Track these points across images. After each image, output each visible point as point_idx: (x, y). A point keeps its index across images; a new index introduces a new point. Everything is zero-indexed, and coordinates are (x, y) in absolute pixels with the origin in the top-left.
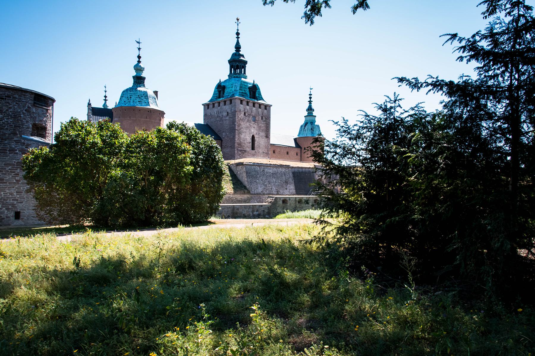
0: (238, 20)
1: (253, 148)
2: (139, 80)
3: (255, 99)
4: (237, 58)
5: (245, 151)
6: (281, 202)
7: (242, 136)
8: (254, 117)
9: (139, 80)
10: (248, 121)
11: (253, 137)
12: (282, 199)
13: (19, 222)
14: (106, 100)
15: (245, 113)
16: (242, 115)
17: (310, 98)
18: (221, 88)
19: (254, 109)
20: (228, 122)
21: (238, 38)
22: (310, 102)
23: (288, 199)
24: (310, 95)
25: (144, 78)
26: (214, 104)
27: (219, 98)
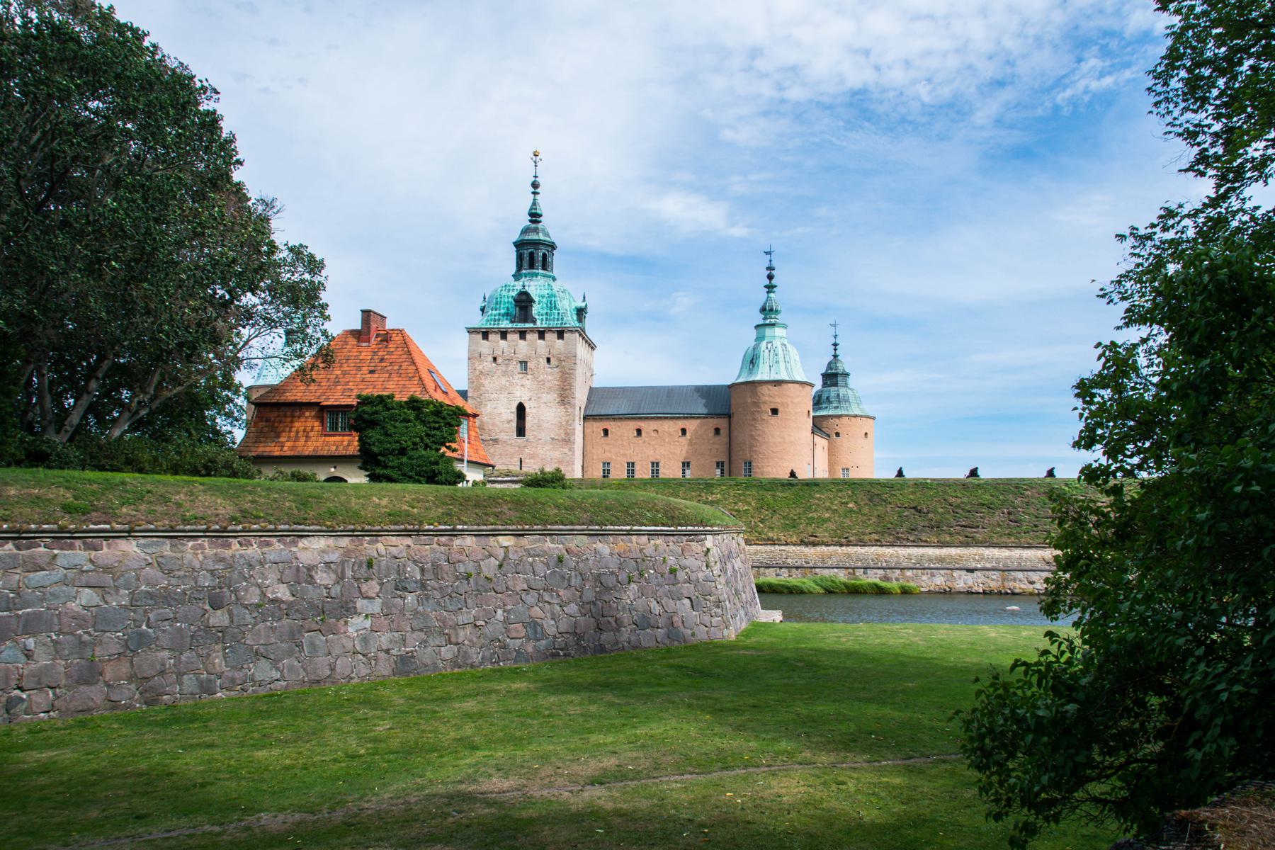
1: (521, 431)
3: (525, 321)
5: (496, 441)
8: (524, 364)
10: (504, 374)
11: (521, 409)
15: (495, 359)
17: (770, 277)
22: (770, 288)
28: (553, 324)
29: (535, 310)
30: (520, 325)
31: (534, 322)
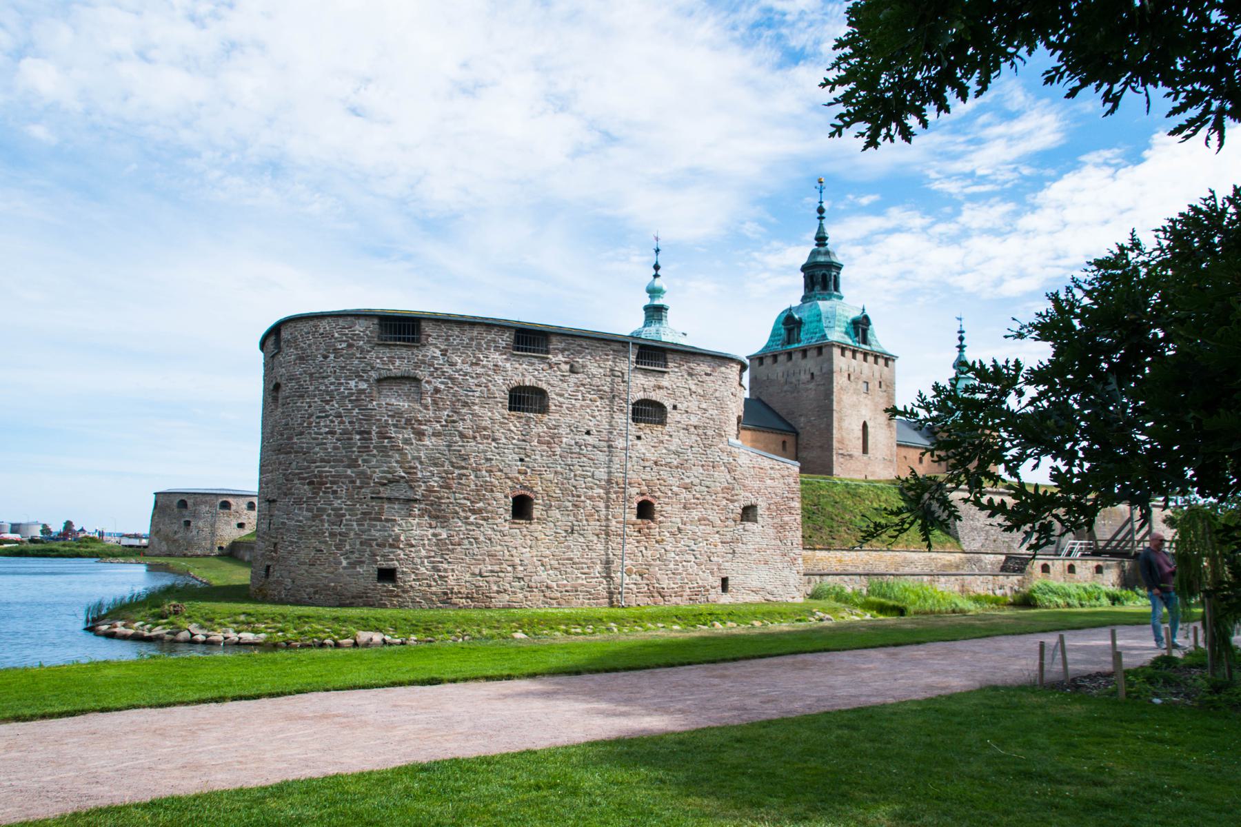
1: (865, 450)
4: (821, 259)
5: (851, 456)
7: (845, 424)
11: (865, 425)
13: (726, 599)
16: (845, 379)
17: (961, 339)
18: (790, 324)
20: (812, 395)
21: (821, 218)
22: (961, 348)
24: (961, 332)
26: (775, 357)
27: (789, 343)
30: (864, 346)
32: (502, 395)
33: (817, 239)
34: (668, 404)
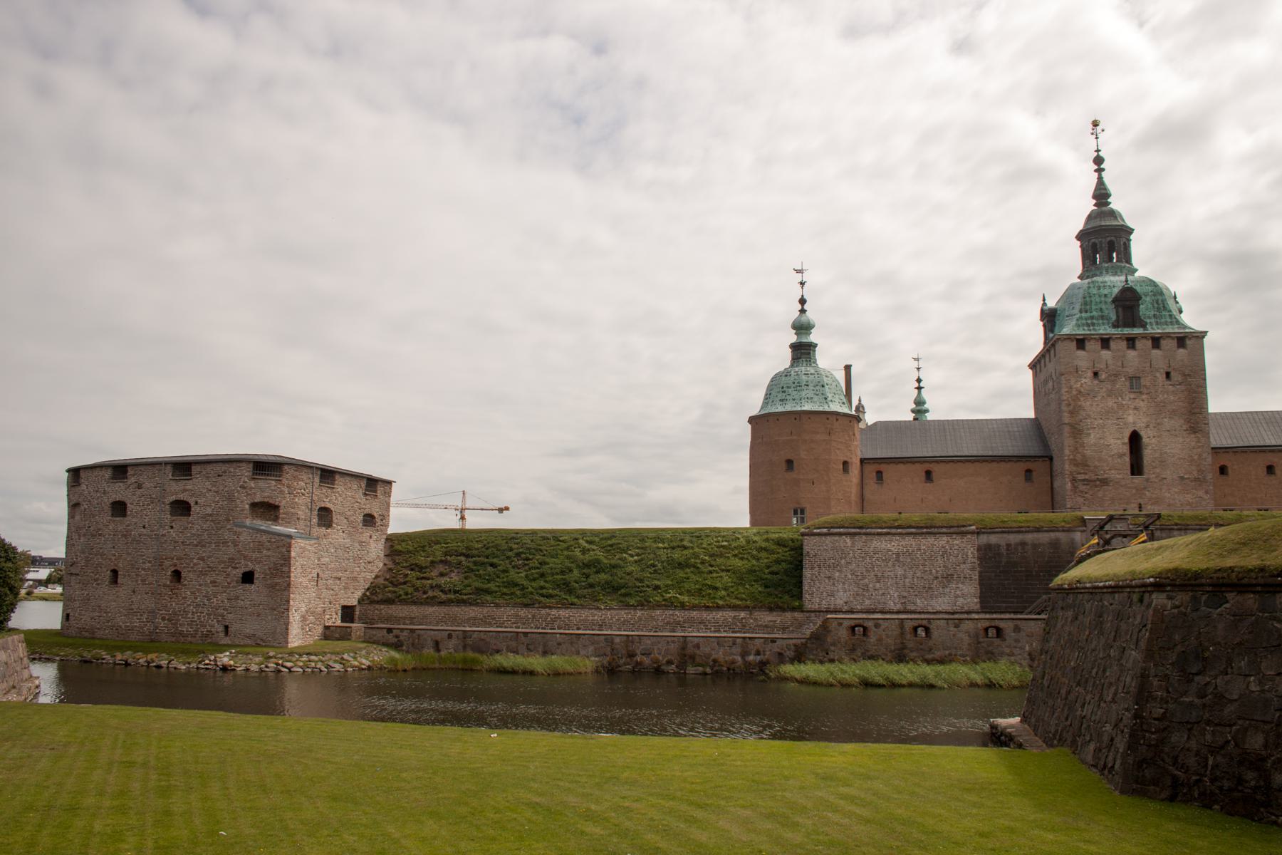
0: (1095, 124)
1: (1136, 467)
2: (803, 351)
3: (1134, 326)
5: (1105, 482)
6: (843, 633)
7: (1092, 439)
8: (1134, 380)
9: (803, 351)
10: (1110, 393)
12: (846, 623)
14: (919, 388)
15: (1096, 374)
16: (1087, 381)
19: (1132, 353)
21: (1099, 171)
23: (870, 624)
25: (816, 345)
28: (1169, 329)
29: (1145, 309)
30: (1127, 331)
31: (1144, 326)
32: (107, 509)
33: (1094, 197)
34: (192, 501)
